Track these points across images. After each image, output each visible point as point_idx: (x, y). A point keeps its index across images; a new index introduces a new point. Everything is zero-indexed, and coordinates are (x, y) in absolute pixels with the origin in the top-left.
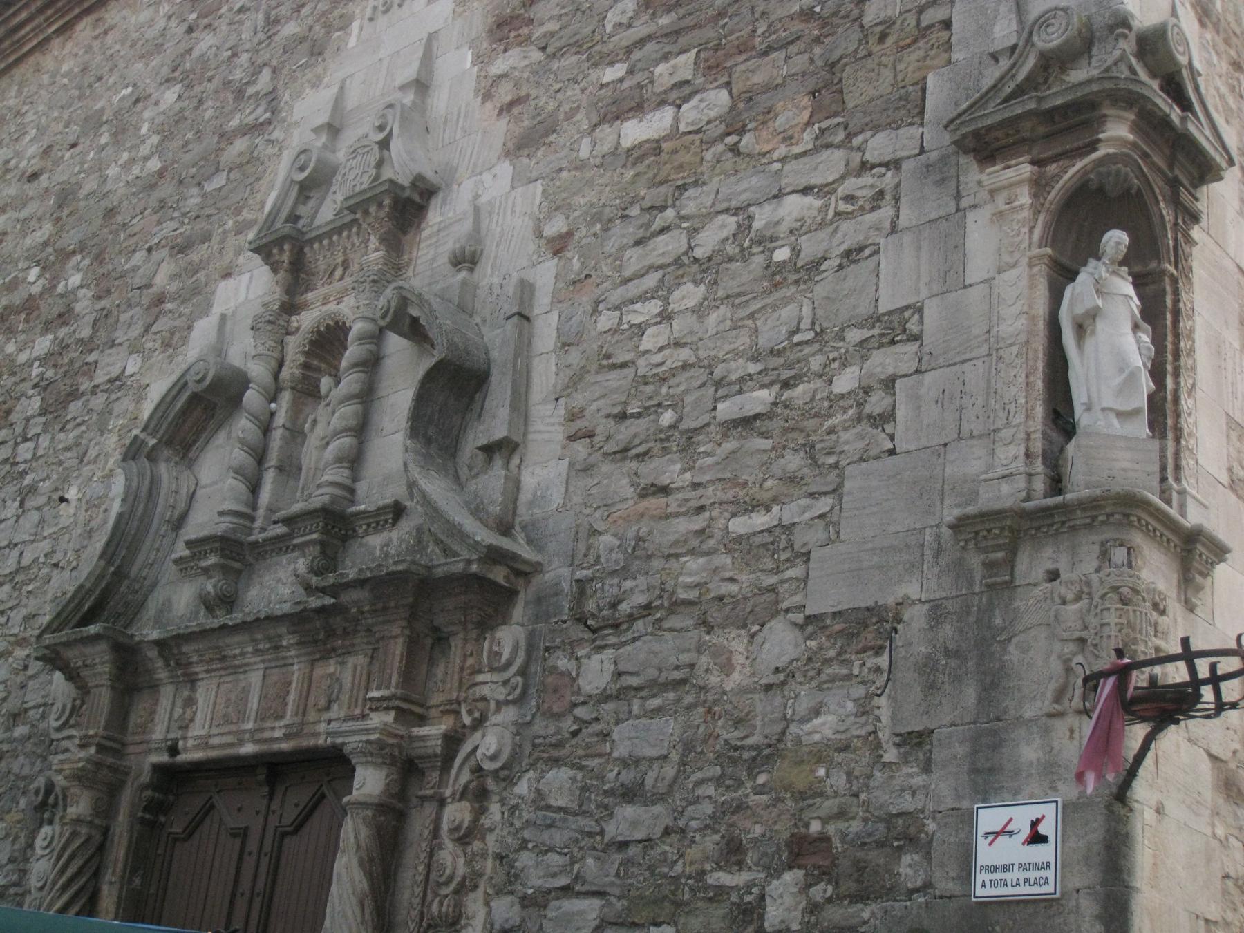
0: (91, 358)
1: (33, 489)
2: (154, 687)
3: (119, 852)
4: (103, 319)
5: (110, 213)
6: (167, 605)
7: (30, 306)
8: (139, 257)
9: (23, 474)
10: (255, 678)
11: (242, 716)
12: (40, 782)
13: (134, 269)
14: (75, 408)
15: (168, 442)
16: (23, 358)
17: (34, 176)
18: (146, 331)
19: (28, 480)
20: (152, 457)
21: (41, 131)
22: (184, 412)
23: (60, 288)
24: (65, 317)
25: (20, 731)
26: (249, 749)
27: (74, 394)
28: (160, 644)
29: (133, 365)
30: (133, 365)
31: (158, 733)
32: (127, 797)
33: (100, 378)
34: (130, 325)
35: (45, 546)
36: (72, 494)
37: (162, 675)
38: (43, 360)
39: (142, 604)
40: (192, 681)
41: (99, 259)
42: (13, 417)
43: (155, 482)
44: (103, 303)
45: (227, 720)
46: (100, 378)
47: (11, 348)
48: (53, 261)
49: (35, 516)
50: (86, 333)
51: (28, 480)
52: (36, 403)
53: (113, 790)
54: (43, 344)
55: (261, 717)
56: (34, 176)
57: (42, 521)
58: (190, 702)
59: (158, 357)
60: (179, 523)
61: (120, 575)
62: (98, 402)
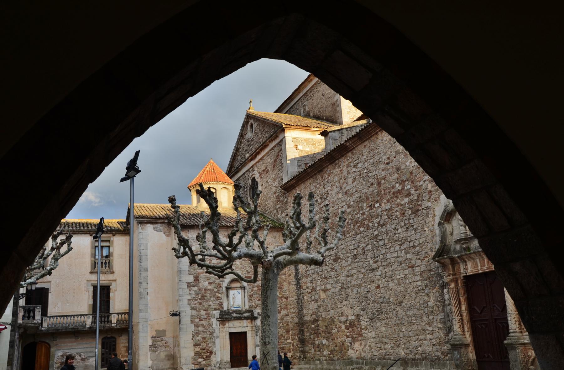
0: (420, 203)
1: (416, 229)
2: (458, 263)
3: (461, 291)
4: (419, 195)
5: (411, 173)
6: (455, 249)
7: (399, 191)
8: (422, 183)
9: (413, 226)
10: (478, 260)
11: (478, 267)
12: (441, 282)
13: (422, 185)
14: (419, 213)
15: (445, 221)
16: (402, 203)
17: (388, 163)
18: (430, 198)
19: (415, 227)
20: (443, 224)
21: (385, 154)
22: (447, 215)
23: (406, 188)
24: (409, 194)
25: (432, 273)
26: (480, 272)
27: (419, 210)
28: (458, 257)
29: (430, 204)
30: (430, 204)
31: (462, 270)
32: (459, 282)
33: (423, 207)
34: (426, 196)
35: (424, 239)
36: (426, 229)
37: (459, 261)
38: (408, 203)
39: (450, 249)
40: (466, 262)
41: (412, 182)
42: (406, 215)
43: (446, 228)
44: (417, 192)
45: (475, 267)
46: (423, 207)
47: (399, 201)
48: (402, 183)
49: (420, 234)
50: (416, 198)
51: (415, 227)
52: (410, 212)
53: (456, 282)
54: (407, 200)
55: (481, 266)
56: (388, 163)
57: (421, 235)
58: (466, 265)
59: (434, 203)
60: (452, 234)
61: (445, 245)
62: (425, 211)
